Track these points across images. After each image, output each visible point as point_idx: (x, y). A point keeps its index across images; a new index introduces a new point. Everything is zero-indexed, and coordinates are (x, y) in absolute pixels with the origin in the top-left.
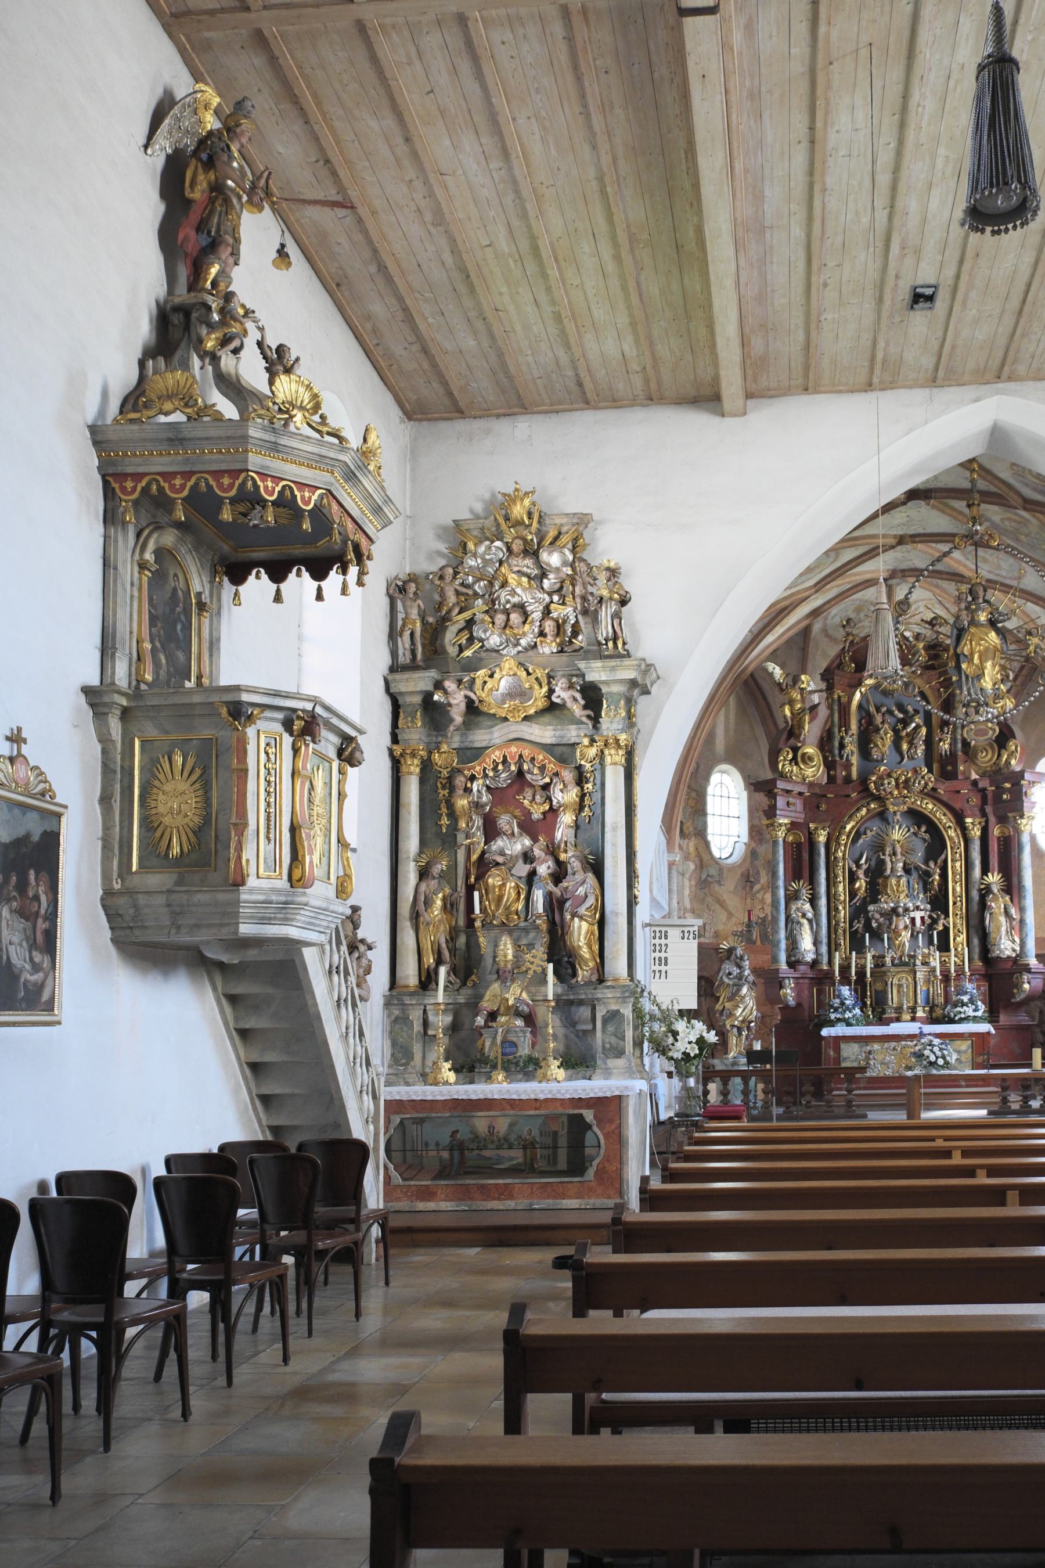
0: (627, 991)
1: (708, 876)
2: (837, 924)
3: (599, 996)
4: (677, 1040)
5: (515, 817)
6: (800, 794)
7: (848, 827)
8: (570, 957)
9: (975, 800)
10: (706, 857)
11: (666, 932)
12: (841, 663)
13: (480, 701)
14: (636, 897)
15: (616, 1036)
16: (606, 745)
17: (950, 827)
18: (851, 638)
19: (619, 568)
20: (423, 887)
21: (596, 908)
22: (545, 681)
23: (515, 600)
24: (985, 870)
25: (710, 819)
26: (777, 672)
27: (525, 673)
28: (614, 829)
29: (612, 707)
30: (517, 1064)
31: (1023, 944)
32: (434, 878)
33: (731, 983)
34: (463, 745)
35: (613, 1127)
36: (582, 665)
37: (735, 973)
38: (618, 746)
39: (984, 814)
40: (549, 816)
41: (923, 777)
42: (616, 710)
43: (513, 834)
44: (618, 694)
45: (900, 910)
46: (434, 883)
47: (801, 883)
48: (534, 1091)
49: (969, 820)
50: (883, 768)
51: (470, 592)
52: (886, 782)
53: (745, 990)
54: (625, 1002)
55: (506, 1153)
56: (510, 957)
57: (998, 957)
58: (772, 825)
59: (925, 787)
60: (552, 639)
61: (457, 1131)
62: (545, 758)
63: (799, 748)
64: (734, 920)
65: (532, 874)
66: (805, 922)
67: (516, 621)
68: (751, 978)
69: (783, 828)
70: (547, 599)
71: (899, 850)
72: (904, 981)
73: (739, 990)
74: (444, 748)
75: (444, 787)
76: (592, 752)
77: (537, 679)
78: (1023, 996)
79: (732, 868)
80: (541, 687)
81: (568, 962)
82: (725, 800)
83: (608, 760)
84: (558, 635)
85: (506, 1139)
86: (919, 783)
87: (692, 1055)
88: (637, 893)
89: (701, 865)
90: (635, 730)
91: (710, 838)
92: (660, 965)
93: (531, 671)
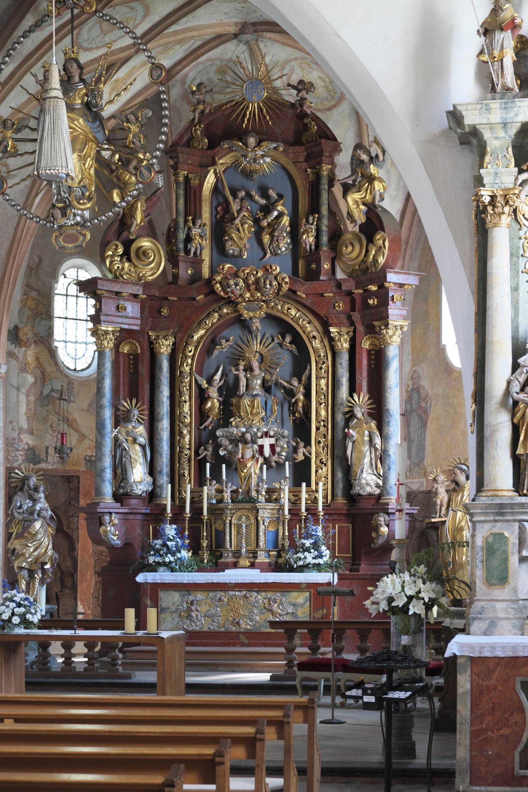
1: (52, 390)
2: (182, 448)
6: (136, 296)
7: (196, 337)
9: (341, 306)
12: (192, 138)
17: (314, 337)
18: (201, 107)
24: (352, 389)
25: (58, 324)
31: (385, 478)
37: (25, 507)
39: (352, 323)
41: (276, 278)
45: (248, 436)
47: (134, 401)
49: (332, 329)
50: (228, 266)
52: (232, 282)
57: (359, 495)
59: (279, 289)
63: (133, 241)
66: (138, 448)
71: (255, 364)
72: (244, 519)
78: (381, 541)
79: (85, 382)
86: (271, 284)
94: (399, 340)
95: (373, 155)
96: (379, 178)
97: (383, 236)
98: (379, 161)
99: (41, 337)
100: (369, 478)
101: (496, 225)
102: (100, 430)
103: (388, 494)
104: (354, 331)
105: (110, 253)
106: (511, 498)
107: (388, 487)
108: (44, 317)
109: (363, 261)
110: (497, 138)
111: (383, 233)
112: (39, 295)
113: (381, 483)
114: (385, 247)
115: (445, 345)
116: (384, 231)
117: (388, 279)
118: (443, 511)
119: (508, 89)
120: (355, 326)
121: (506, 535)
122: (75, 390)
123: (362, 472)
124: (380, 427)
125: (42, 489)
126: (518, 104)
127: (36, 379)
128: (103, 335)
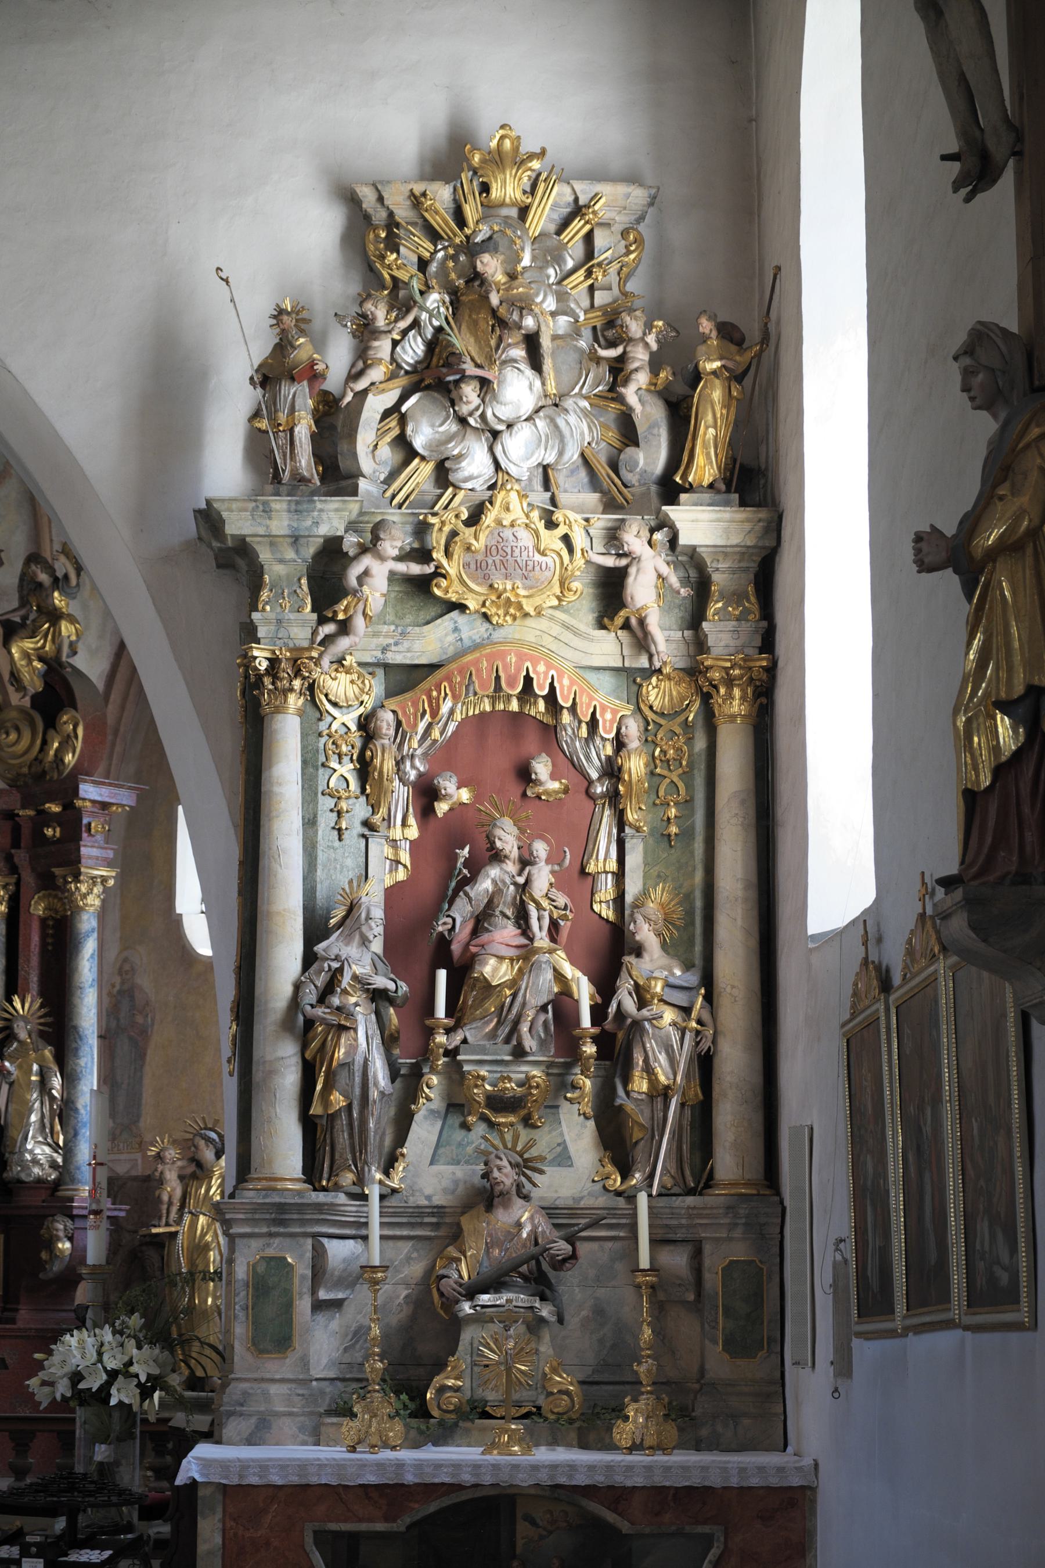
31: (68, 1151)
39: (14, 869)
57: (20, 1181)
78: (57, 1267)
94: (97, 902)
95: (60, 574)
96: (69, 615)
97: (74, 717)
98: (69, 586)
100: (38, 1151)
101: (280, 710)
103: (73, 1180)
104: (18, 884)
106: (299, 1193)
107: (72, 1167)
109: (36, 759)
110: (281, 561)
111: (73, 712)
113: (60, 1160)
114: (76, 737)
115: (181, 915)
116: (76, 709)
117: (82, 794)
118: (173, 1215)
119: (303, 480)
120: (19, 875)
121: (290, 1260)
123: (26, 1138)
124: (61, 1059)
126: (319, 505)
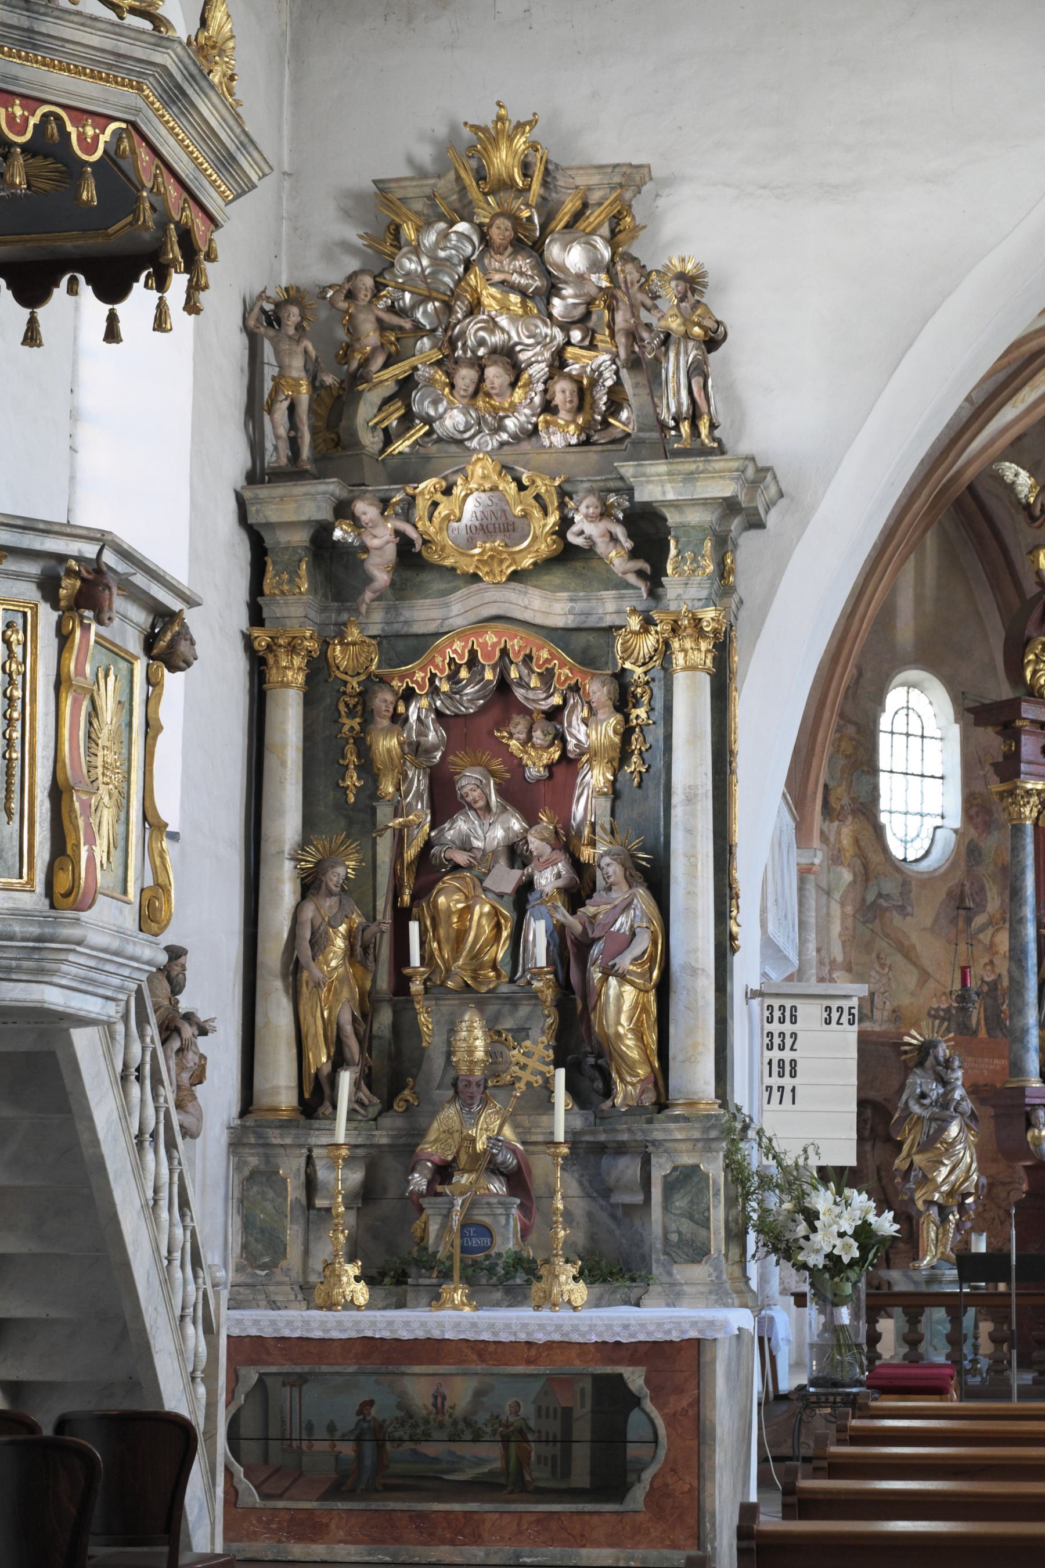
0: (713, 1127)
3: (658, 1135)
4: (814, 1230)
5: (493, 774)
8: (599, 1056)
10: (875, 858)
11: (794, 1008)
13: (425, 542)
14: (733, 938)
15: (691, 1218)
16: (675, 630)
19: (703, 275)
20: (309, 911)
21: (652, 959)
22: (553, 502)
23: (496, 339)
26: (1024, 481)
27: (513, 485)
28: (691, 799)
29: (688, 554)
30: (491, 1270)
32: (330, 894)
33: (926, 1114)
34: (392, 629)
35: (684, 1403)
36: (628, 469)
37: (934, 1095)
38: (699, 632)
40: (559, 771)
42: (694, 560)
43: (488, 807)
44: (700, 528)
46: (329, 905)
48: (525, 1326)
51: (407, 325)
53: (954, 1130)
54: (710, 1150)
55: (467, 1450)
56: (480, 1054)
58: (1011, 793)
60: (568, 417)
61: (371, 1403)
62: (553, 656)
64: (931, 985)
65: (527, 887)
67: (497, 382)
68: (968, 1106)
69: (1034, 799)
70: (560, 337)
73: (943, 1129)
74: (354, 634)
75: (351, 714)
76: (648, 643)
77: (538, 497)
79: (929, 880)
80: (546, 514)
81: (596, 1067)
82: (914, 742)
83: (679, 659)
84: (580, 409)
85: (468, 1422)
87: (846, 1260)
88: (735, 929)
89: (866, 874)
90: (733, 601)
91: (884, 818)
92: (781, 1075)
93: (525, 481)
99: (861, 803)
102: (1020, 960)
105: (1032, 657)
108: (866, 768)
112: (858, 731)
122: (913, 895)
125: (957, 1063)
127: (855, 875)
128: (1022, 797)
